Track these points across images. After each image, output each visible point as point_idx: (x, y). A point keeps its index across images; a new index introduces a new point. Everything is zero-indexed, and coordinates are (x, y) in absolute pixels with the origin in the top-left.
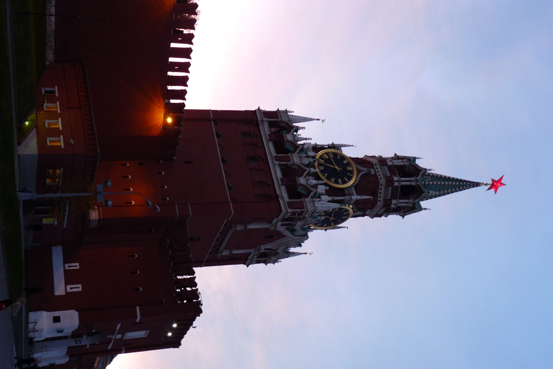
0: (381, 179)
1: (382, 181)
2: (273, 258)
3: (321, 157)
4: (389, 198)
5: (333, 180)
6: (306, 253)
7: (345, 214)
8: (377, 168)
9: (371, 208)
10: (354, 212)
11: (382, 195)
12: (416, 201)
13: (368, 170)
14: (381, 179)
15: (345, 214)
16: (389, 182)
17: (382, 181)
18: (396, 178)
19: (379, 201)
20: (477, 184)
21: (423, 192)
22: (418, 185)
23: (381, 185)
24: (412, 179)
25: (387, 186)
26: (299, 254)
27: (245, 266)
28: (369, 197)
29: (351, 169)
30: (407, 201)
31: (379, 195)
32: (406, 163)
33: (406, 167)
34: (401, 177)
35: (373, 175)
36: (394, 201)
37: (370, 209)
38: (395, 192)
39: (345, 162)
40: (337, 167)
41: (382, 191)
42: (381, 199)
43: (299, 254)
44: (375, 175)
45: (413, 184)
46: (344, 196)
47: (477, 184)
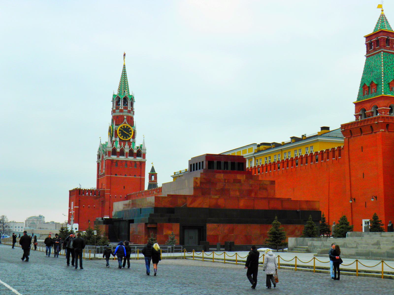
2: (142, 151)
4: (118, 111)
6: (144, 137)
7: (123, 128)
9: (123, 116)
10: (125, 123)
11: (118, 114)
15: (123, 128)
20: (124, 66)
22: (116, 99)
23: (115, 114)
26: (144, 140)
28: (114, 121)
33: (117, 100)
36: (120, 108)
37: (124, 117)
41: (117, 114)
43: (144, 140)
47: (124, 66)
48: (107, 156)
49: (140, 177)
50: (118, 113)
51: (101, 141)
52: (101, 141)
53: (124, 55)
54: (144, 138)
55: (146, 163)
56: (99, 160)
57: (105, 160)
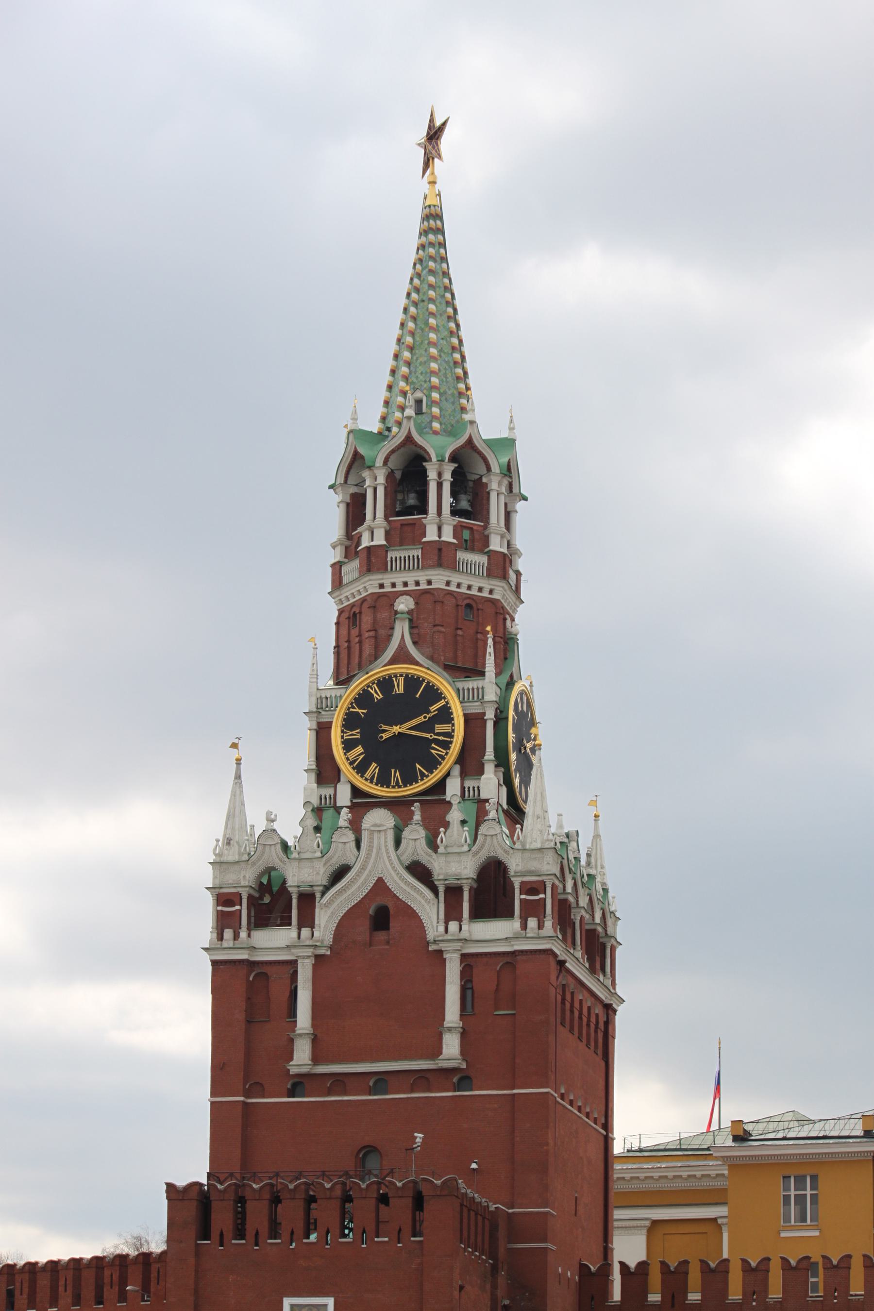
0: (429, 583)
1: (439, 579)
3: (361, 769)
4: (483, 559)
5: (436, 751)
7: (520, 708)
8: (394, 585)
11: (476, 583)
12: (495, 469)
13: (402, 619)
14: (429, 583)
16: (440, 556)
17: (439, 579)
18: (431, 535)
19: (491, 592)
20: (433, 220)
21: (470, 442)
23: (448, 583)
24: (432, 475)
25: (453, 566)
26: (597, 836)
27: (621, 1010)
29: (402, 680)
30: (493, 496)
31: (474, 592)
32: (381, 480)
34: (424, 510)
35: (416, 603)
36: (496, 544)
38: (466, 535)
39: (378, 696)
40: (396, 729)
41: (465, 581)
42: (487, 584)
43: (597, 836)
44: (420, 596)
45: (447, 476)
46: (485, 721)
47: (433, 220)
48: (548, 923)
49: (605, 1133)
50: (469, 578)
51: (238, 777)
52: (238, 777)
53: (434, 134)
54: (596, 827)
55: (618, 1018)
56: (249, 936)
57: (464, 957)
